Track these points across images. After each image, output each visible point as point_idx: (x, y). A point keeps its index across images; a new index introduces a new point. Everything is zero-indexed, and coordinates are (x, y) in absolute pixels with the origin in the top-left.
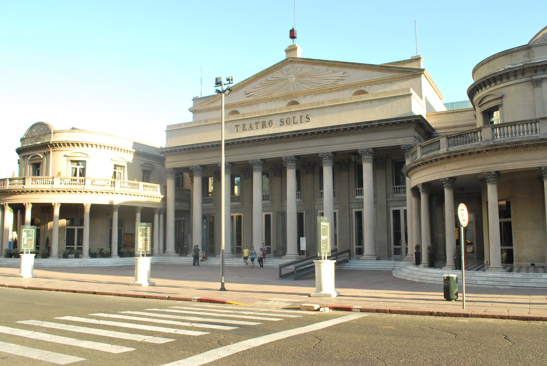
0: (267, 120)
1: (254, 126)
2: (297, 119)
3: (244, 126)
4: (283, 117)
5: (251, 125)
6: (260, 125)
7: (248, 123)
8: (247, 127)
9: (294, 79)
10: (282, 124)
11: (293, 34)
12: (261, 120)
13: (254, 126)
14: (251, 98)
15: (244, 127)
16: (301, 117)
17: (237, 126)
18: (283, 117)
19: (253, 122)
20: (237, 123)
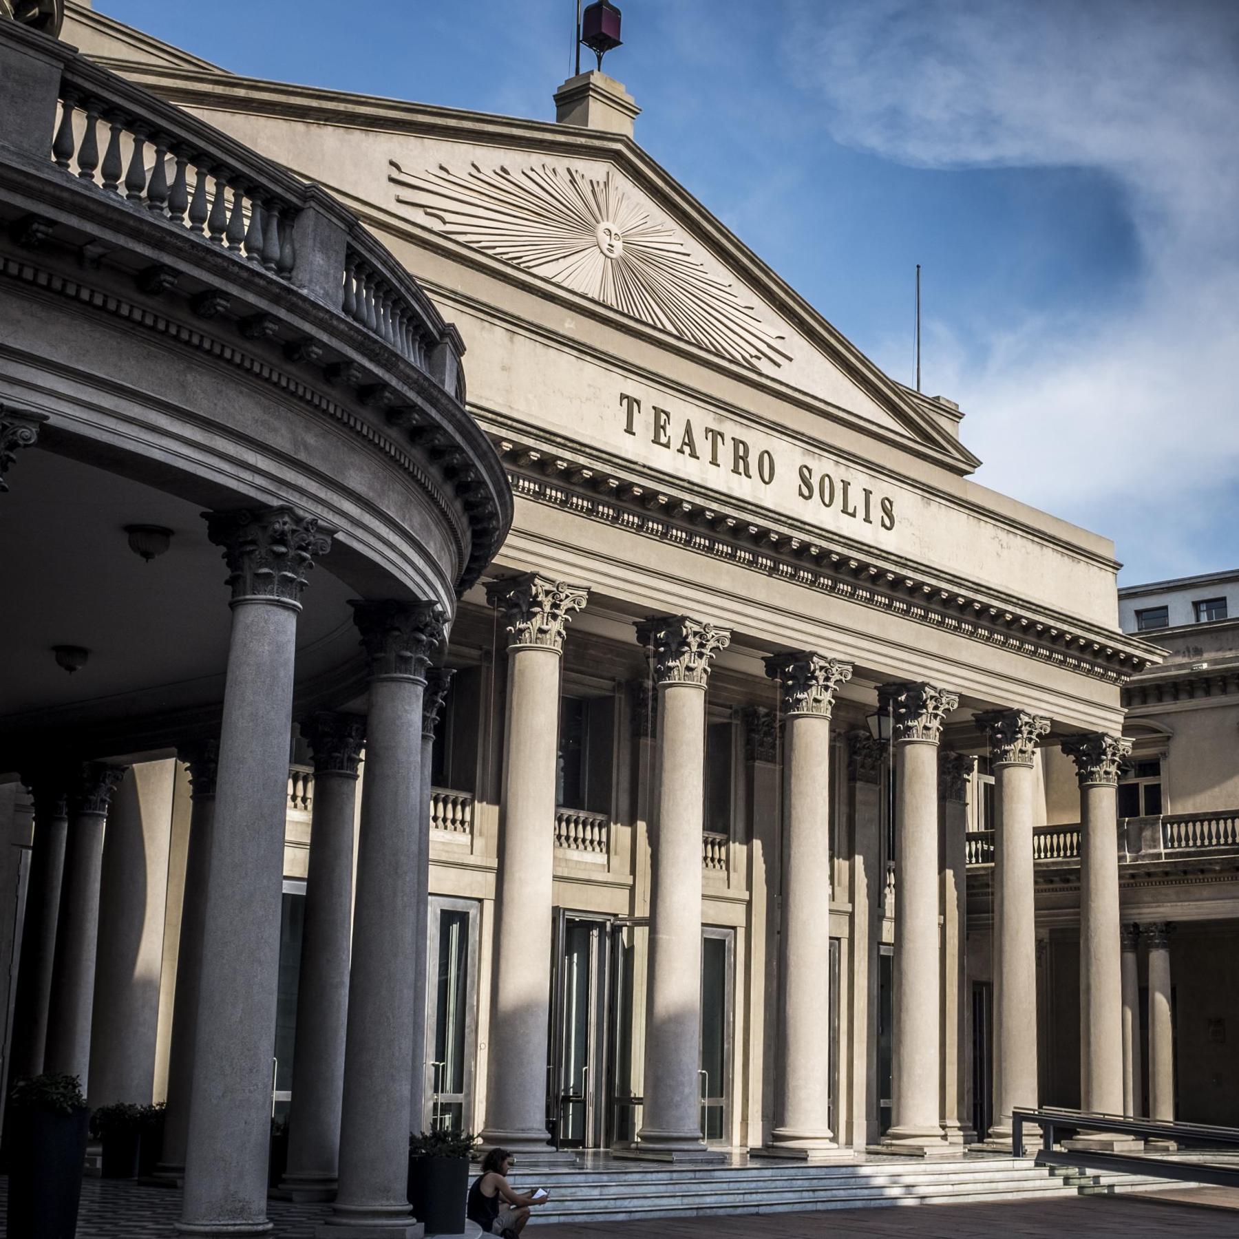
0: (757, 440)
1: (703, 446)
2: (856, 499)
3: (660, 419)
4: (812, 463)
5: (688, 431)
6: (726, 452)
7: (681, 411)
8: (675, 432)
9: (618, 245)
10: (806, 493)
11: (599, 31)
12: (731, 429)
13: (703, 446)
14: (418, 216)
15: (659, 428)
16: (868, 493)
17: (631, 403)
18: (812, 463)
19: (702, 418)
20: (634, 387)
